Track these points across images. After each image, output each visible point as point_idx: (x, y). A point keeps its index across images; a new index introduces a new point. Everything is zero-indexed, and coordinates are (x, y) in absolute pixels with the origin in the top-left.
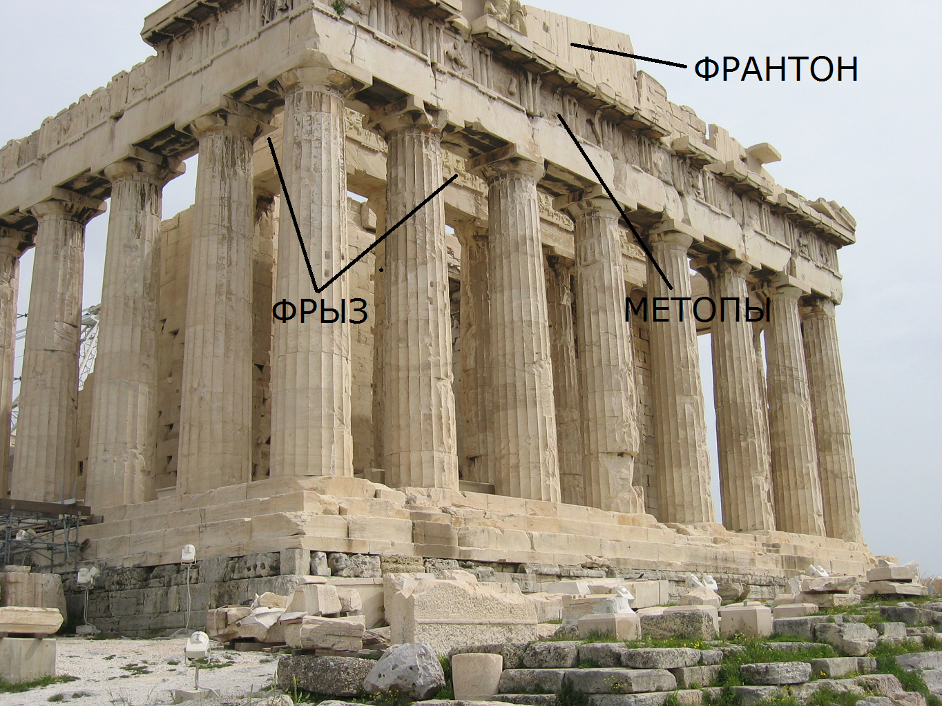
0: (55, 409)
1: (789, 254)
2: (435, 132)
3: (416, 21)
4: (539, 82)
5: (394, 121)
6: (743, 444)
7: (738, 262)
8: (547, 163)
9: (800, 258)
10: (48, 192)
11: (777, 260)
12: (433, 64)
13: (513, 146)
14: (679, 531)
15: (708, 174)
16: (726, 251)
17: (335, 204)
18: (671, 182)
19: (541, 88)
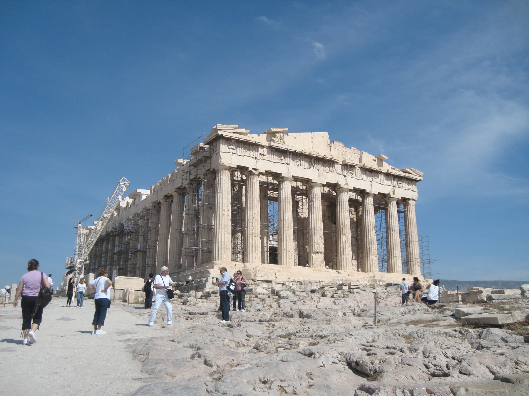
1: (392, 187)
2: (256, 175)
4: (291, 155)
7: (369, 193)
8: (293, 176)
11: (386, 190)
12: (256, 158)
14: (339, 273)
16: (365, 190)
18: (341, 173)
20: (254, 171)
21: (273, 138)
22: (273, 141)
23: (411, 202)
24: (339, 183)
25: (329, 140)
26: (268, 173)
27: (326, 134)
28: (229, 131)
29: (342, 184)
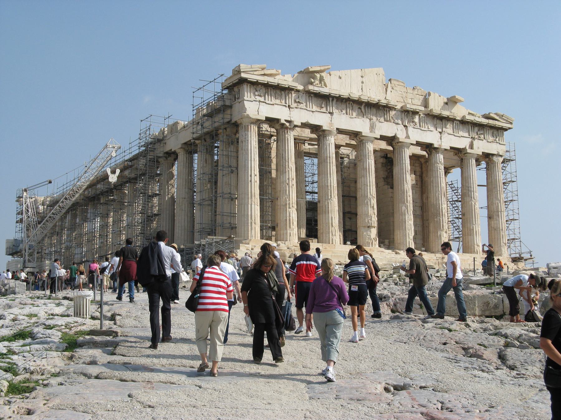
0: (186, 217)
1: (470, 140)
2: (290, 129)
3: (283, 92)
5: (278, 126)
6: (436, 219)
7: (437, 148)
8: (337, 129)
9: (476, 140)
10: (180, 146)
12: (289, 106)
13: (322, 126)
14: (396, 253)
15: (422, 115)
16: (431, 145)
17: (253, 159)
19: (336, 101)
20: (288, 124)
21: (313, 80)
22: (312, 83)
23: (495, 158)
24: (398, 136)
25: (384, 78)
26: (305, 125)
27: (381, 70)
28: (255, 73)
29: (401, 136)
